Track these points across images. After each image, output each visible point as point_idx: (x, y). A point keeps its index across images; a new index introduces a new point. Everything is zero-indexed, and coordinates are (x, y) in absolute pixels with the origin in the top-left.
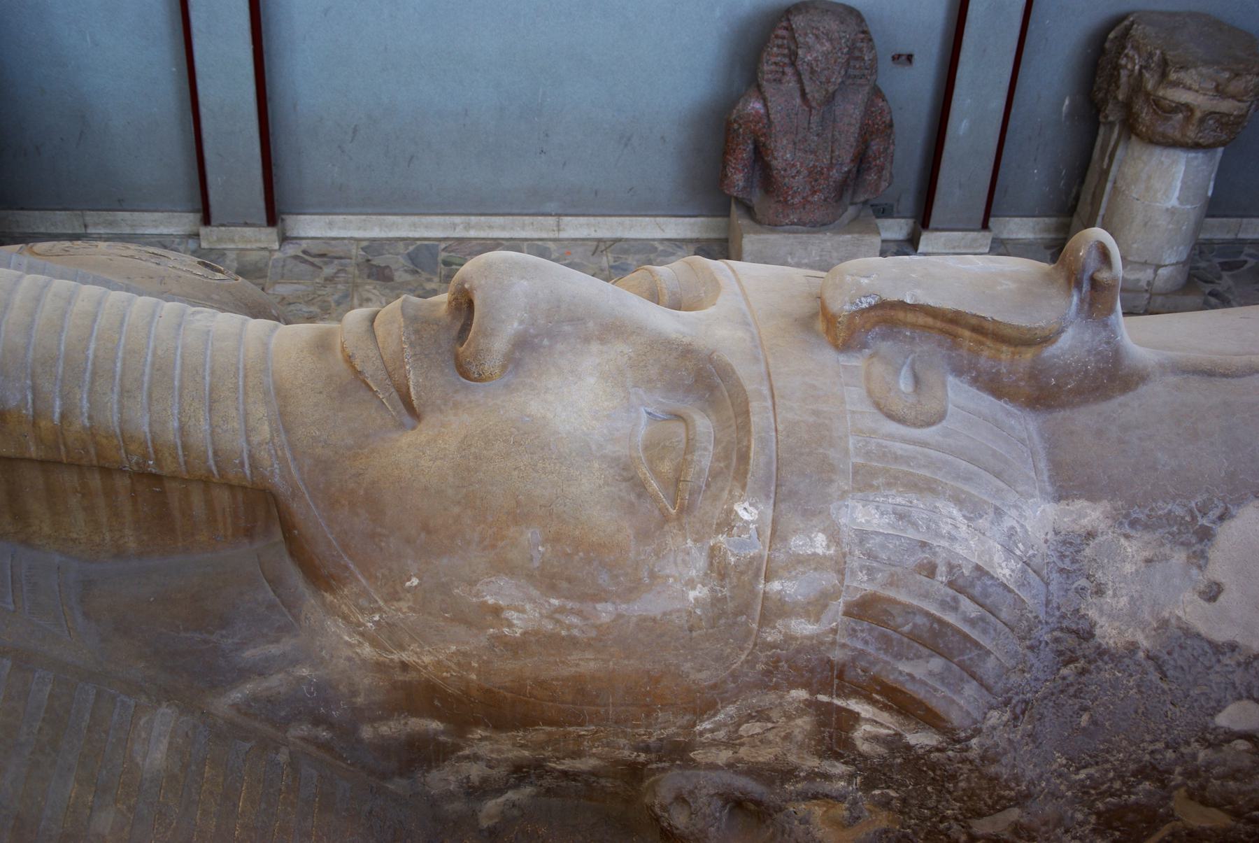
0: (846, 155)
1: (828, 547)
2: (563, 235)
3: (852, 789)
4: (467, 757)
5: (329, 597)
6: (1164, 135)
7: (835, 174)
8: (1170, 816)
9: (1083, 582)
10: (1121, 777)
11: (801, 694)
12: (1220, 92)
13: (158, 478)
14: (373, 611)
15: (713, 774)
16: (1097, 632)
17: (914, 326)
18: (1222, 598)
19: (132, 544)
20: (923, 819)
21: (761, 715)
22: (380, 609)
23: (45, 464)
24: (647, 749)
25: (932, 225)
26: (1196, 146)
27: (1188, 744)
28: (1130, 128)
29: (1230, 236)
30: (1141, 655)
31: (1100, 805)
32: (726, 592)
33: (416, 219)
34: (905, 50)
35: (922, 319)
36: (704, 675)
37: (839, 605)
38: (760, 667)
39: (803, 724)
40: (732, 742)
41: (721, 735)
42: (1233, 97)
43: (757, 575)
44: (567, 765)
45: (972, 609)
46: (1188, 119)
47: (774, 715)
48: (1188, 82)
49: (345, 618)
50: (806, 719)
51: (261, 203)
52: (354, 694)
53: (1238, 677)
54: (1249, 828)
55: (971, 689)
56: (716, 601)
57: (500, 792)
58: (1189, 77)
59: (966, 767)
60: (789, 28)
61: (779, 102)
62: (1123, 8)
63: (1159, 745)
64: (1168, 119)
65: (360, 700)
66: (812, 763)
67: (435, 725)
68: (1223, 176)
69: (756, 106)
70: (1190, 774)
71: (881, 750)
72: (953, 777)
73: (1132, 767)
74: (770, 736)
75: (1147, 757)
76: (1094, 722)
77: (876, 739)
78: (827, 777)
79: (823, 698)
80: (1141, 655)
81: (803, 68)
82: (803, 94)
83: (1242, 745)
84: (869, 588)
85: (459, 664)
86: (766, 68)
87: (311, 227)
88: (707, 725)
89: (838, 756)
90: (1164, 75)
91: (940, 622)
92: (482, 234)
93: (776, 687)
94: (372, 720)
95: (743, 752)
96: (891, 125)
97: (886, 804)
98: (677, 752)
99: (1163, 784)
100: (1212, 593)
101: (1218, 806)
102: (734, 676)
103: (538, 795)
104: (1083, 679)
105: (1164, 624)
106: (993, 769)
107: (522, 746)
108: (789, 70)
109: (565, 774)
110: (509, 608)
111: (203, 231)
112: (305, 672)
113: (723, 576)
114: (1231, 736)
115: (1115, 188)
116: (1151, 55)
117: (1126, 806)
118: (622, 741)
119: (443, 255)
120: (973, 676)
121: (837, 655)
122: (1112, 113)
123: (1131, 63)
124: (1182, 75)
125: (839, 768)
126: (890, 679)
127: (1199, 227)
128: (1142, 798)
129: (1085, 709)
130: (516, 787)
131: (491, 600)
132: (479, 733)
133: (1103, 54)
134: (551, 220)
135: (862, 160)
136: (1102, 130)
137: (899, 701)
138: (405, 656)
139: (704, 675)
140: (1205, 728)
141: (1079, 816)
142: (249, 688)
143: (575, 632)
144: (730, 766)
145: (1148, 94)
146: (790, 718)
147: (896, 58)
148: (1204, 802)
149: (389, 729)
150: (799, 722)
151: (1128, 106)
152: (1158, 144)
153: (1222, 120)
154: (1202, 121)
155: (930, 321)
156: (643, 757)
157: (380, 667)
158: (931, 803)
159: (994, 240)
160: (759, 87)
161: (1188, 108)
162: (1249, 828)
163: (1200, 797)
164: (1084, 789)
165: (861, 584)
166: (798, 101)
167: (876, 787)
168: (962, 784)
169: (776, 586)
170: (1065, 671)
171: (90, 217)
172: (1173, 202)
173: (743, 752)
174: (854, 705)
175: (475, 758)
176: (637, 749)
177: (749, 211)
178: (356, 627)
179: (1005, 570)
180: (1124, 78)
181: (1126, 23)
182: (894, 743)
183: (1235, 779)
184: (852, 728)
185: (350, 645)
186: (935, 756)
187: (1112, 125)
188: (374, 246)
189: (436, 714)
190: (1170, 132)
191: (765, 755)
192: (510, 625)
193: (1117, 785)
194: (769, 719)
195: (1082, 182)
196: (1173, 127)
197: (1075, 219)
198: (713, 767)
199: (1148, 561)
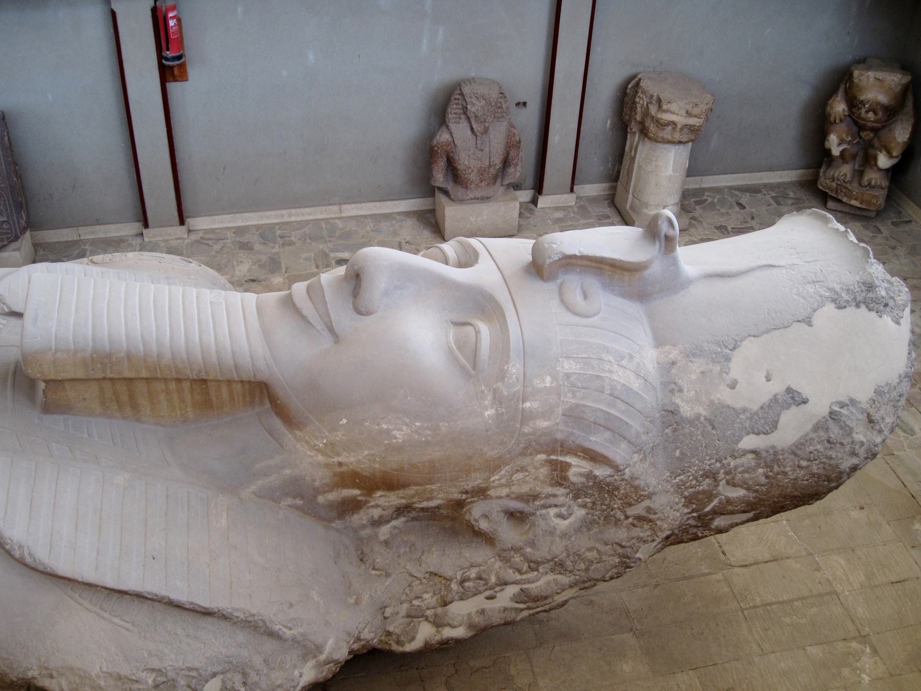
0: (498, 161)
1: (552, 383)
2: (344, 215)
3: (568, 500)
4: (373, 507)
5: (298, 433)
6: (663, 138)
7: (493, 171)
8: (719, 494)
9: (673, 386)
10: (696, 479)
11: (542, 457)
12: (689, 114)
13: (205, 381)
14: (323, 438)
15: (499, 501)
16: (681, 410)
17: (580, 266)
18: (738, 387)
19: (191, 416)
20: (604, 510)
21: (522, 469)
22: (327, 437)
23: (147, 380)
24: (466, 492)
25: (544, 190)
26: (680, 142)
27: (726, 458)
28: (644, 132)
29: (697, 186)
30: (702, 419)
31: (686, 493)
32: (503, 410)
33: (261, 213)
34: (522, 101)
35: (585, 262)
36: (495, 452)
37: (560, 410)
38: (522, 446)
39: (544, 471)
40: (508, 484)
41: (503, 481)
42: (696, 116)
43: (518, 400)
44: (425, 504)
45: (622, 406)
46: (674, 129)
47: (529, 469)
48: (672, 109)
49: (307, 442)
50: (545, 468)
51: (176, 214)
52: (314, 481)
53: (747, 424)
54: (754, 495)
55: (624, 445)
56: (498, 416)
57: (388, 522)
58: (674, 107)
59: (624, 483)
60: (462, 94)
61: (459, 132)
62: (633, 71)
63: (713, 461)
64: (663, 129)
65: (317, 484)
66: (550, 490)
67: (356, 492)
68: (692, 157)
70: (726, 473)
71: (583, 480)
72: (617, 489)
73: (701, 473)
74: (527, 479)
75: (708, 467)
76: (682, 453)
77: (581, 475)
78: (555, 496)
79: (553, 457)
80: (702, 419)
82: (472, 129)
83: (751, 456)
84: (573, 401)
85: (369, 460)
86: (450, 116)
87: (201, 223)
88: (497, 477)
89: (561, 485)
90: (660, 107)
91: (608, 413)
92: (299, 219)
93: (531, 454)
94: (324, 492)
95: (514, 488)
96: (520, 142)
97: (584, 506)
98: (481, 493)
99: (715, 480)
100: (733, 385)
101: (741, 487)
102: (510, 453)
103: (407, 521)
104: (676, 433)
105: (712, 403)
106: (636, 483)
107: (402, 498)
108: (463, 117)
109: (423, 509)
110: (394, 430)
111: (145, 231)
112: (288, 471)
113: (501, 403)
114: (745, 452)
115: (640, 167)
116: (652, 96)
117: (698, 492)
118: (454, 490)
119: (279, 232)
120: (625, 438)
121: (559, 436)
122: (634, 127)
124: (669, 106)
125: (561, 491)
126: (587, 445)
127: (684, 183)
128: (706, 488)
129: (677, 448)
130: (397, 518)
131: (384, 426)
132: (379, 493)
133: (627, 99)
134: (336, 208)
135: (506, 163)
136: (629, 136)
137: (593, 457)
138: (340, 459)
139: (495, 452)
140: (734, 450)
141: (677, 500)
142: (259, 483)
143: (430, 438)
144: (508, 496)
145: (653, 117)
146: (537, 469)
147: (518, 104)
148: (734, 485)
149: (333, 496)
150: (542, 470)
151: (642, 123)
152: (660, 142)
153: (692, 129)
154: (681, 129)
155: (589, 263)
156: (464, 496)
157: (327, 466)
158: (607, 502)
159: (577, 198)
160: (447, 126)
161: (674, 123)
162: (754, 495)
163: (731, 483)
164: (679, 486)
165: (570, 400)
166: (469, 133)
167: (579, 498)
168: (622, 491)
169: (528, 405)
170: (667, 431)
171: (82, 230)
172: (670, 172)
173: (514, 488)
174: (569, 459)
175: (377, 506)
176: (462, 493)
177: (445, 192)
178: (314, 448)
179: (636, 384)
180: (639, 109)
181: (637, 79)
182: (589, 476)
183: (748, 472)
184: (568, 470)
185: (309, 456)
186: (608, 480)
187: (634, 133)
188: (240, 231)
189: (358, 486)
190: (666, 136)
191: (525, 489)
192: (396, 438)
193: (694, 482)
194: (527, 471)
195: (621, 163)
196: (667, 133)
197: (619, 183)
198: (500, 498)
199: (703, 373)
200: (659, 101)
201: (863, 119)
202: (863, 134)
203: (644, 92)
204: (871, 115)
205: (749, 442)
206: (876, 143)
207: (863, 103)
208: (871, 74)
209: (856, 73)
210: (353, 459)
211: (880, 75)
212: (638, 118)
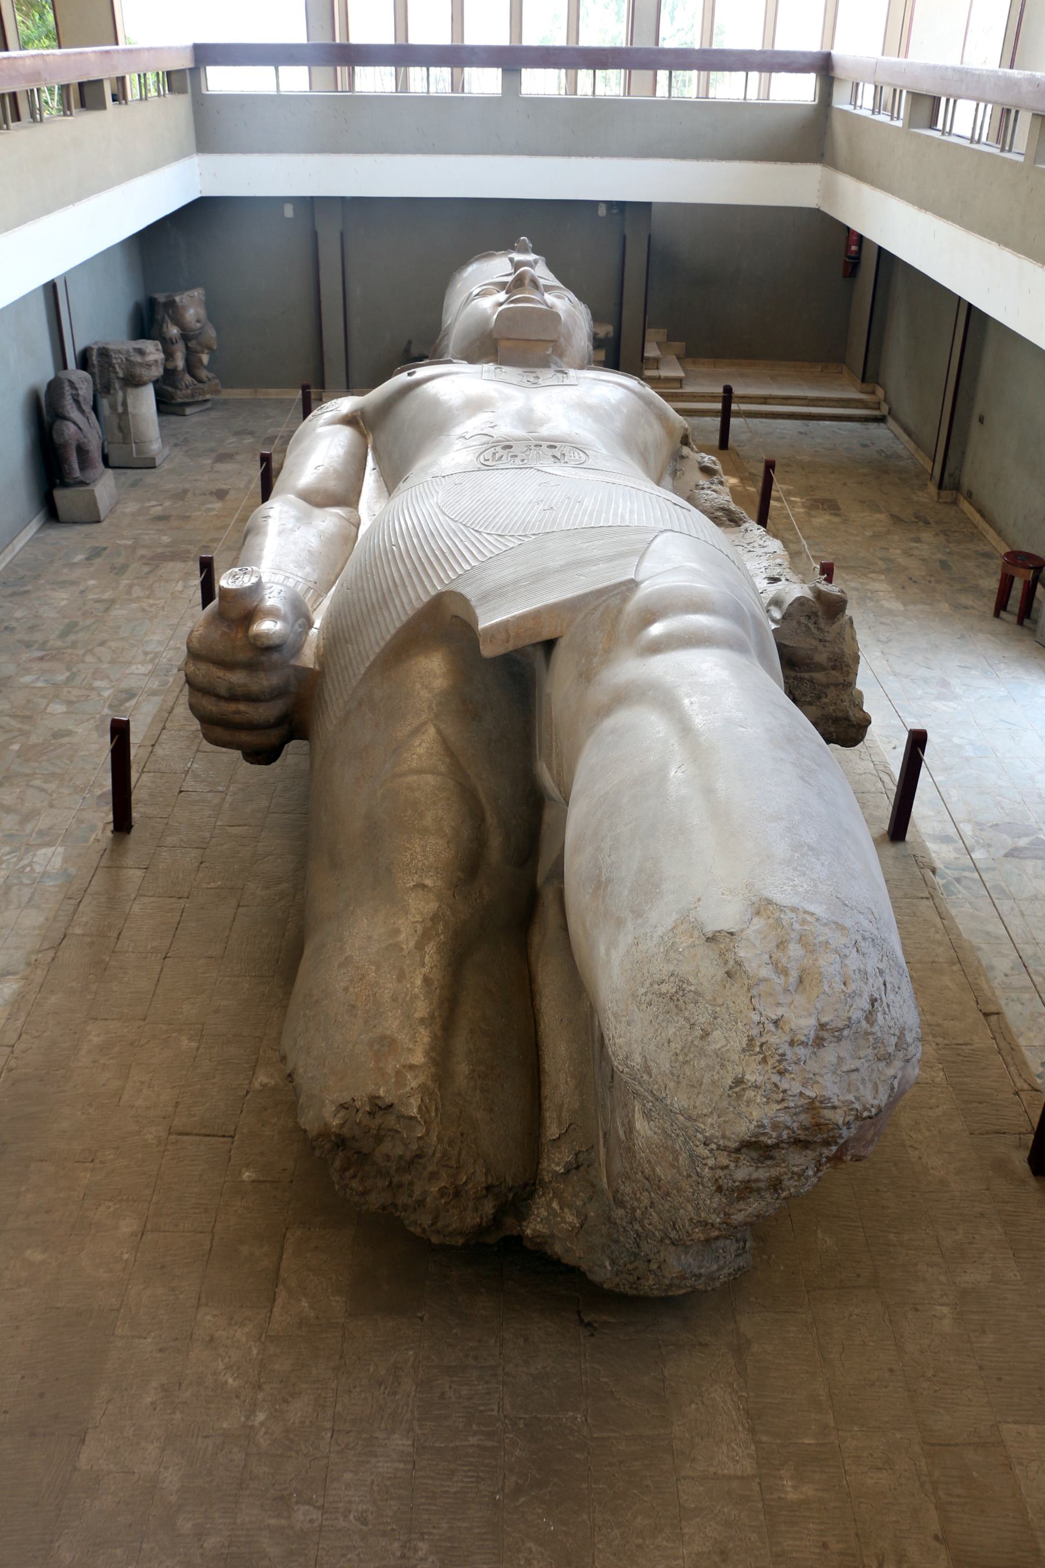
60: (72, 384)
69: (72, 428)
81: (81, 399)
108: (74, 405)
115: (134, 416)
122: (117, 386)
145: (141, 364)
161: (156, 361)
181: (95, 353)
202: (192, 344)
203: (119, 352)
204: (198, 325)
206: (199, 348)
209: (177, 299)
212: (121, 375)
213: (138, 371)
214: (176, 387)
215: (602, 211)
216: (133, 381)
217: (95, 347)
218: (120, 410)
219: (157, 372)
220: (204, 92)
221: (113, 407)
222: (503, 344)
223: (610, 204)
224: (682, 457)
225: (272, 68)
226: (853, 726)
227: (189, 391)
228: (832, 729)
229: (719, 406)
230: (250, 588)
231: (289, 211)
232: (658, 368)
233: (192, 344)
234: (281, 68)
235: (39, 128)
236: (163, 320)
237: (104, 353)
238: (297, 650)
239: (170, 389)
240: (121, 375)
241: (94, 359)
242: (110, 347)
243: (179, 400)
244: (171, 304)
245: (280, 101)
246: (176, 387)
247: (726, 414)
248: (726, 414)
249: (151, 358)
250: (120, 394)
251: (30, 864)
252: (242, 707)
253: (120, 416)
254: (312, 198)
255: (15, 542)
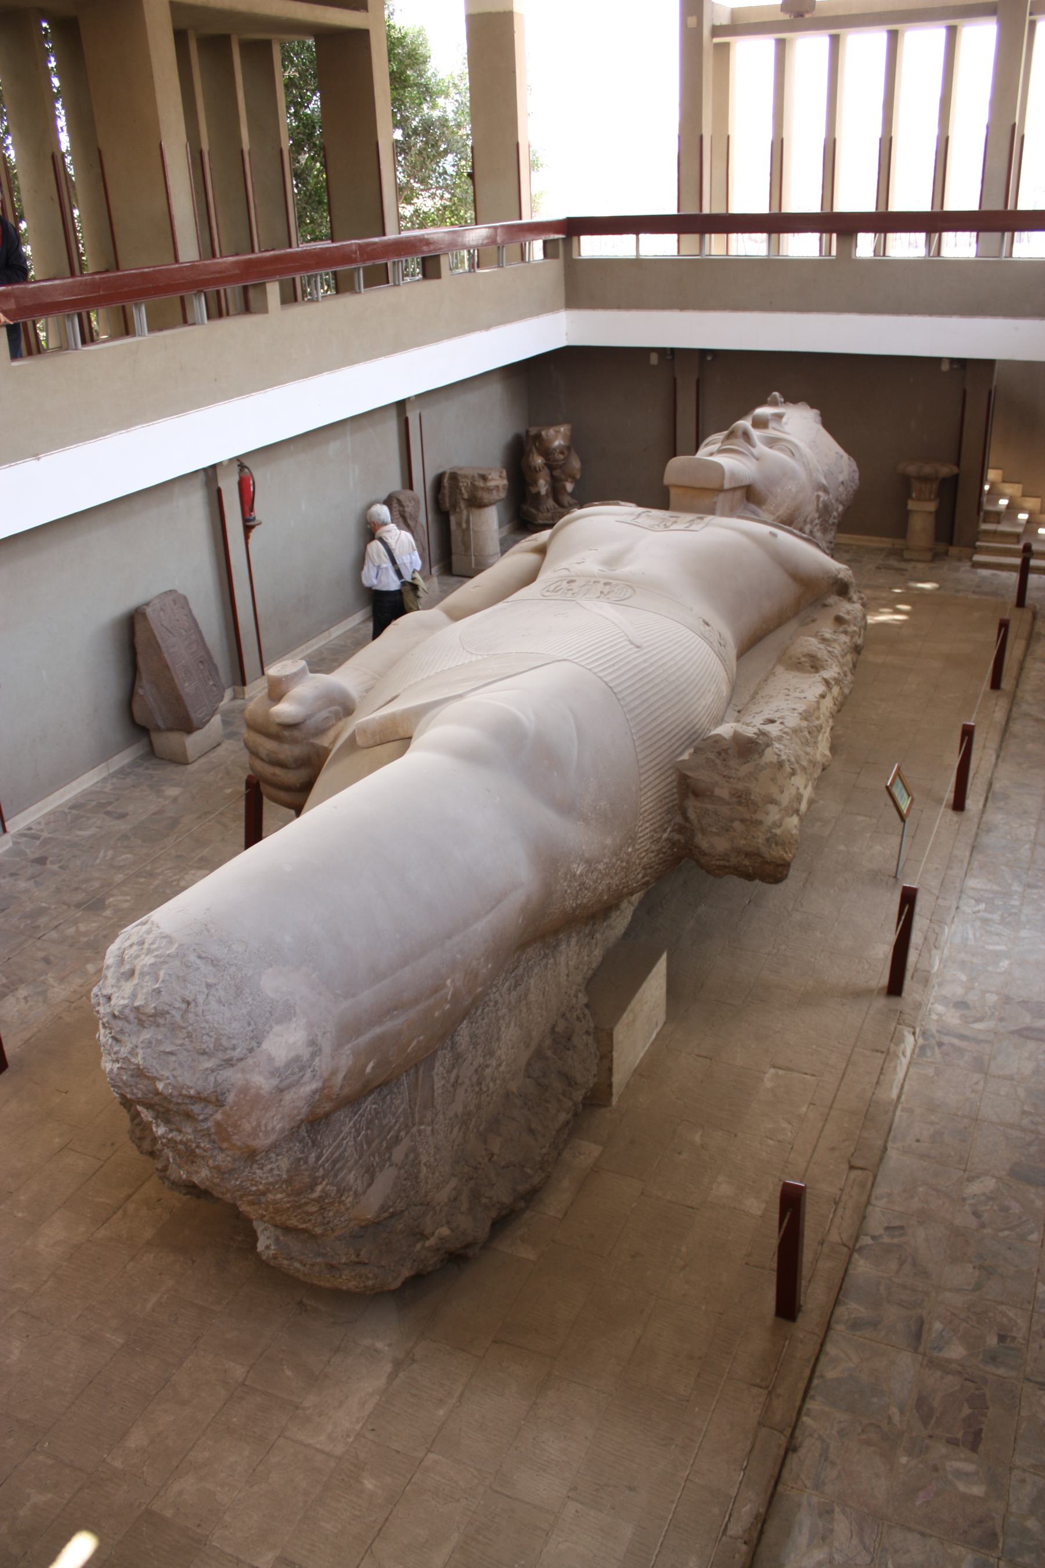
60: (399, 502)
81: (407, 515)
115: (475, 532)
122: (462, 505)
123: (463, 484)
136: (453, 519)
138: (778, 514)
145: (483, 489)
161: (497, 487)
174: (821, 493)
187: (461, 512)
197: (454, 558)
200: (484, 478)
201: (558, 461)
203: (466, 477)
204: (561, 457)
205: (841, 478)
206: (563, 477)
207: (555, 449)
208: (552, 431)
209: (543, 433)
210: (782, 511)
211: (557, 428)
213: (480, 494)
214: (538, 510)
215: (945, 367)
216: (476, 503)
217: (448, 471)
218: (464, 526)
219: (503, 495)
220: (575, 256)
221: (459, 524)
222: (673, 492)
223: (953, 361)
224: (825, 606)
225: (634, 236)
226: (767, 863)
227: (550, 514)
228: (747, 862)
229: (1017, 561)
230: (286, 676)
231: (654, 359)
232: (999, 523)
233: (557, 473)
234: (642, 236)
235: (396, 289)
236: (530, 451)
237: (454, 477)
238: (321, 731)
239: (533, 511)
240: (466, 496)
241: (446, 481)
242: (459, 472)
243: (540, 522)
244: (538, 437)
245: (637, 264)
246: (538, 510)
247: (1025, 570)
248: (1025, 570)
249: (492, 484)
250: (465, 513)
251: (178, 880)
252: (278, 771)
253: (463, 531)
254: (673, 350)
255: (332, 630)
